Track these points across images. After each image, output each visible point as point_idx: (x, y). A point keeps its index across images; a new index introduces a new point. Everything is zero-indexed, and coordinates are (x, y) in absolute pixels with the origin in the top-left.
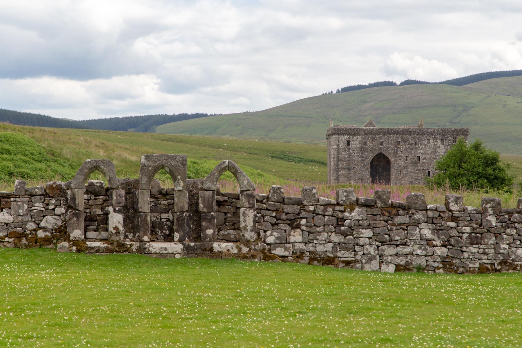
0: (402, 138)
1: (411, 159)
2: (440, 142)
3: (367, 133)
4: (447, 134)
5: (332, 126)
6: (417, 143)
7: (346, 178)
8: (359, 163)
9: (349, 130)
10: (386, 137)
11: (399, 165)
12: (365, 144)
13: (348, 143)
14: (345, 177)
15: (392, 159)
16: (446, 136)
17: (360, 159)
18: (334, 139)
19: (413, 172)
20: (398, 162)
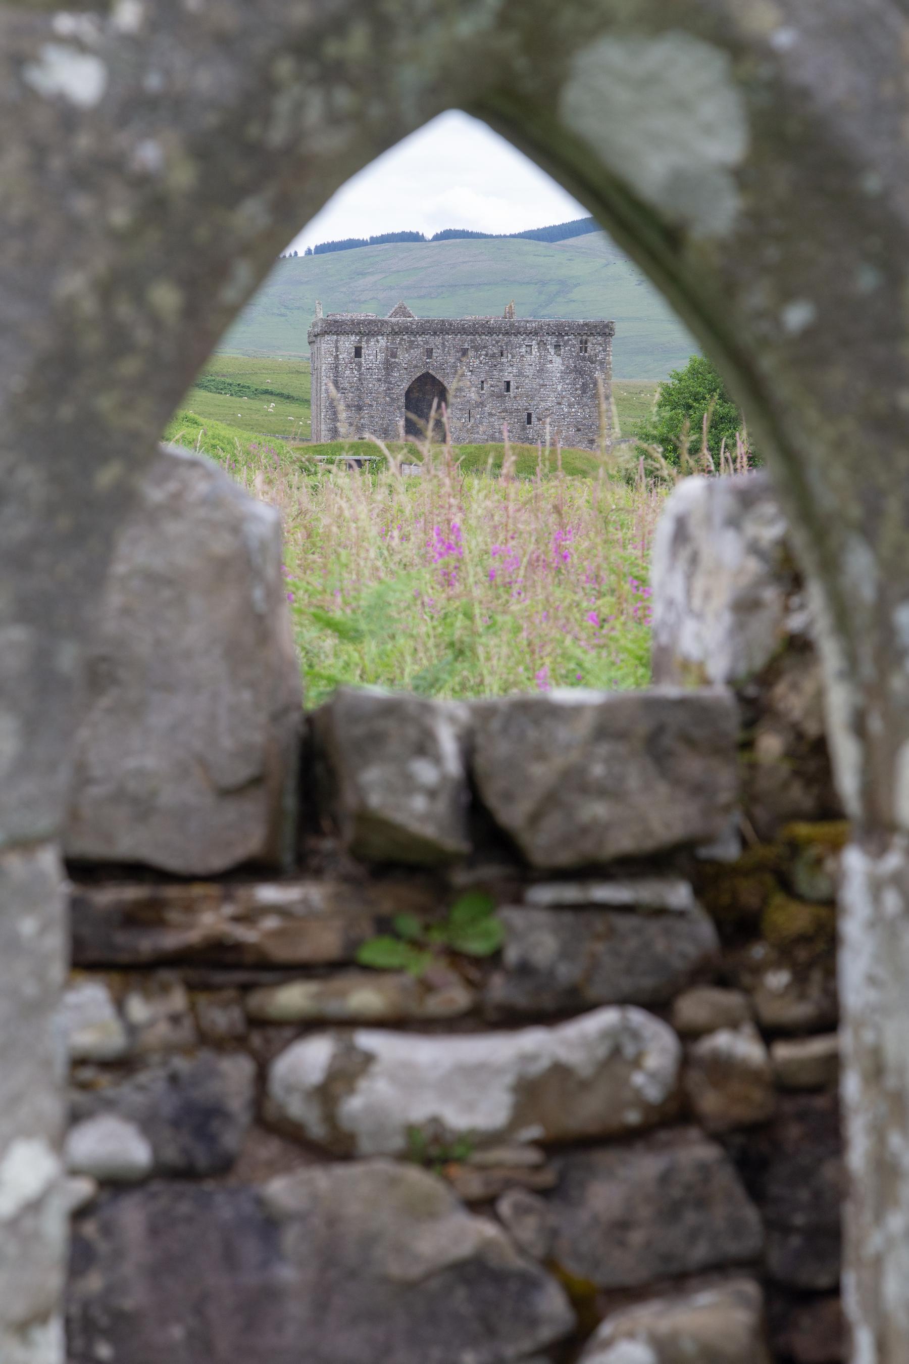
0: (471, 341)
1: (492, 386)
2: (552, 351)
3: (397, 331)
4: (567, 334)
5: (321, 315)
6: (505, 352)
9: (359, 324)
10: (438, 340)
11: (466, 399)
12: (394, 355)
13: (358, 352)
16: (566, 338)
17: (383, 387)
18: (326, 344)
19: (495, 415)
20: (463, 394)
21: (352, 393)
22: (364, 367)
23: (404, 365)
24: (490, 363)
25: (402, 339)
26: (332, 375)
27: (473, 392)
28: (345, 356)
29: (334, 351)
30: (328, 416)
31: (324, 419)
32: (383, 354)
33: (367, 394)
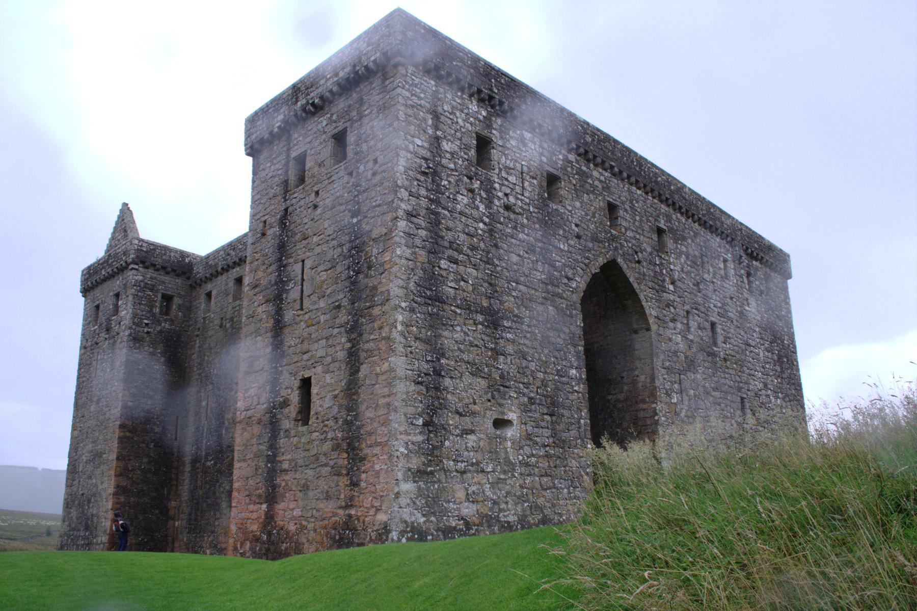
1: (699, 328)
7: (483, 383)
8: (538, 295)
15: (652, 311)
21: (475, 266)
22: (499, 199)
23: (573, 226)
24: (693, 275)
26: (423, 192)
27: (680, 334)
28: (456, 149)
29: (430, 122)
30: (414, 329)
32: (535, 182)
33: (509, 282)
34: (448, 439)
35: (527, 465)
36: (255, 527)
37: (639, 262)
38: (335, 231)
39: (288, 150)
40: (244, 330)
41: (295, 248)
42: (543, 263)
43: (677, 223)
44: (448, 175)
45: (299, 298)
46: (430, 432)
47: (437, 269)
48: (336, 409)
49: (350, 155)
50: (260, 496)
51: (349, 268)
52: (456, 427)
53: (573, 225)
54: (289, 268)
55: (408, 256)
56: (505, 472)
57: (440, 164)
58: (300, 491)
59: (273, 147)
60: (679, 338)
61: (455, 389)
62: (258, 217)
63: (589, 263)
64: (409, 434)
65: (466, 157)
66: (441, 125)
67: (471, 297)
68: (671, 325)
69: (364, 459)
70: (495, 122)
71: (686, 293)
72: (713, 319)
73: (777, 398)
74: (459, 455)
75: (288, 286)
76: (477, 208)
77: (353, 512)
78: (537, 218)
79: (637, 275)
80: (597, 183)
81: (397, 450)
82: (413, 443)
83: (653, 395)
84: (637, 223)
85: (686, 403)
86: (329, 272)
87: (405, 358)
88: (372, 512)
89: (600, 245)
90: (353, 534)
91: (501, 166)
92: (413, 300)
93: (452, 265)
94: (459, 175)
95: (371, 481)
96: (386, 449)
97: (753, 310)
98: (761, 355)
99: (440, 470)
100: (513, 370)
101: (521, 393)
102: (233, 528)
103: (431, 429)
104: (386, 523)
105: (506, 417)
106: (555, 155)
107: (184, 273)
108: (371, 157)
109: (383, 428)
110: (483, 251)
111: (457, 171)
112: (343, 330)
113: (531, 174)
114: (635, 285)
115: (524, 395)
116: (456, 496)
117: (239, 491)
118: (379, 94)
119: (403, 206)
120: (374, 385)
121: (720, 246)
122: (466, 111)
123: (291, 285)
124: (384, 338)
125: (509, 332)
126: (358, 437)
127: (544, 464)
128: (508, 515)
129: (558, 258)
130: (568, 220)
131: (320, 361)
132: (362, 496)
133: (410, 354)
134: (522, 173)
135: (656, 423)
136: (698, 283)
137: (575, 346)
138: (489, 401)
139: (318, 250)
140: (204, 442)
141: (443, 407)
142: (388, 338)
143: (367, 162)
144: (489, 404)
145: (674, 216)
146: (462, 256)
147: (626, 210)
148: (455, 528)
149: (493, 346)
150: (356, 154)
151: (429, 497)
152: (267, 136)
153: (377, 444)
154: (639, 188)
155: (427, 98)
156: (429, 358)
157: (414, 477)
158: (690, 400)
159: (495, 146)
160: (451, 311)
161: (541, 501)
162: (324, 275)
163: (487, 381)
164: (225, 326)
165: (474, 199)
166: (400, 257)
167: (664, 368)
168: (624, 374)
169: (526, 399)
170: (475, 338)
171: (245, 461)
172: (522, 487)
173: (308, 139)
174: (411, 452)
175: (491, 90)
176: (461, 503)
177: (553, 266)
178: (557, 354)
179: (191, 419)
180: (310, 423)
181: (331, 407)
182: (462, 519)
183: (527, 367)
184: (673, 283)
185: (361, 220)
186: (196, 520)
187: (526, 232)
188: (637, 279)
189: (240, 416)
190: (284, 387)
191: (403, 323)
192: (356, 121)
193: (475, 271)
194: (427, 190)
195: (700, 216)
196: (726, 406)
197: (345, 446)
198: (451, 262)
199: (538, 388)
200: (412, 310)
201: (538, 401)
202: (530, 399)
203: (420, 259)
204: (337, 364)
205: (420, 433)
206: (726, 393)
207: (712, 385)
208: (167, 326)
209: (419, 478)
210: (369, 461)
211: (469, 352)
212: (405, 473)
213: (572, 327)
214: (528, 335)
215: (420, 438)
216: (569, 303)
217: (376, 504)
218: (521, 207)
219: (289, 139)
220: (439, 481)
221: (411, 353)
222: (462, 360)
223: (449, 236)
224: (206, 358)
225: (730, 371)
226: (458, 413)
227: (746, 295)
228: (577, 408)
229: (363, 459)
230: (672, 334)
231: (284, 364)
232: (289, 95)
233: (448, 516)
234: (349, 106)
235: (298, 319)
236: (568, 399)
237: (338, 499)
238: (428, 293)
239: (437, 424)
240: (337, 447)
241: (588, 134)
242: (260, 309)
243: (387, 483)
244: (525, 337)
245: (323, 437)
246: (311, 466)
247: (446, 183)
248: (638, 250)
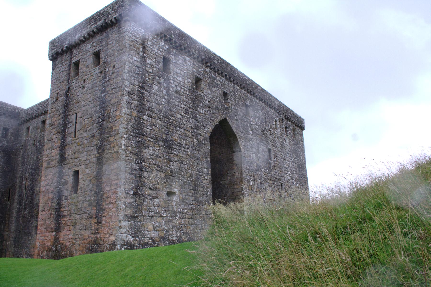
1: (263, 151)
7: (163, 174)
14: (159, 169)
15: (242, 143)
22: (173, 88)
23: (207, 102)
25: (205, 71)
26: (136, 83)
27: (254, 154)
28: (153, 63)
29: (141, 49)
30: (130, 148)
31: (124, 150)
32: (190, 80)
34: (145, 201)
35: (182, 213)
36: (49, 244)
37: (237, 120)
38: (93, 100)
39: (71, 59)
40: (46, 147)
41: (72, 107)
42: (192, 119)
43: (255, 103)
44: (149, 75)
45: (74, 131)
46: (136, 197)
47: (142, 120)
48: (91, 186)
49: (102, 63)
50: (52, 228)
51: (99, 118)
52: (149, 195)
53: (207, 102)
54: (69, 117)
55: (128, 113)
56: (172, 217)
57: (145, 69)
58: (72, 226)
59: (63, 57)
60: (254, 156)
61: (149, 177)
62: (54, 91)
63: (214, 120)
64: (126, 198)
65: (158, 67)
66: (146, 51)
67: (158, 134)
68: (251, 149)
69: (104, 210)
70: (173, 51)
71: (258, 135)
72: (270, 147)
73: (297, 183)
74: (150, 209)
75: (69, 125)
76: (162, 92)
77: (98, 236)
78: (190, 98)
79: (235, 126)
80: (219, 82)
81: (120, 206)
82: (128, 203)
83: (241, 182)
84: (236, 102)
85: (256, 185)
86: (89, 119)
87: (125, 162)
88: (108, 236)
89: (219, 111)
90: (98, 246)
91: (174, 72)
92: (130, 134)
93: (149, 118)
94: (154, 75)
95: (108, 221)
96: (115, 205)
97: (287, 144)
98: (290, 164)
99: (141, 215)
100: (177, 169)
101: (180, 179)
102: (38, 244)
103: (137, 196)
104: (114, 241)
105: (173, 191)
106: (200, 68)
107: (15, 117)
108: (112, 65)
109: (114, 195)
110: (164, 112)
111: (153, 74)
112: (95, 147)
113: (188, 77)
114: (235, 131)
115: (182, 180)
116: (149, 228)
117: (41, 226)
118: (117, 34)
119: (127, 89)
120: (110, 174)
121: (274, 114)
122: (158, 45)
123: (70, 125)
124: (115, 152)
125: (175, 151)
126: (102, 199)
127: (190, 213)
128: (173, 237)
129: (199, 117)
130: (205, 99)
131: (83, 162)
132: (103, 228)
133: (128, 160)
134: (184, 76)
135: (243, 194)
136: (263, 130)
137: (206, 158)
138: (165, 183)
139: (84, 108)
140: (24, 202)
141: (143, 185)
142: (117, 152)
143: (110, 67)
144: (165, 184)
145: (253, 100)
146: (154, 114)
147: (232, 96)
148: (148, 243)
149: (167, 157)
150: (104, 63)
151: (135, 228)
152: (60, 51)
153: (111, 203)
154: (238, 86)
155: (140, 38)
156: (137, 162)
157: (128, 219)
158: (258, 184)
159: (172, 62)
160: (148, 140)
161: (188, 230)
162: (87, 121)
163: (164, 173)
164: (36, 144)
165: (161, 87)
166: (124, 113)
167: (247, 169)
168: (229, 172)
169: (182, 183)
170: (159, 153)
171: (44, 211)
172: (179, 224)
173: (81, 54)
174: (127, 207)
175: (171, 36)
176: (151, 231)
177: (197, 120)
178: (197, 161)
179: (17, 190)
180: (78, 193)
181: (88, 185)
182: (151, 239)
183: (183, 167)
184: (252, 130)
185: (106, 95)
186: (18, 241)
187: (185, 104)
188: (236, 128)
189: (42, 189)
190: (65, 175)
191: (125, 145)
192: (105, 47)
193: (160, 121)
194: (139, 82)
195: (265, 100)
196: (274, 187)
197: (95, 204)
198: (148, 117)
199: (188, 177)
200: (129, 139)
201: (188, 184)
202: (184, 182)
203: (134, 115)
204: (92, 164)
205: (132, 198)
206: (274, 181)
207: (268, 178)
208: (5, 143)
209: (131, 219)
210: (107, 211)
211: (156, 159)
212: (124, 217)
213: (205, 149)
214: (184, 153)
215: (132, 200)
216: (204, 138)
217: (110, 232)
218: (183, 92)
219: (71, 53)
220: (140, 221)
221: (128, 159)
222: (153, 163)
223: (148, 104)
224: (26, 160)
225: (277, 171)
226: (150, 188)
227: (285, 137)
228: (206, 187)
229: (104, 210)
230: (251, 154)
231: (66, 163)
232: (72, 32)
233: (145, 237)
234: (102, 39)
235: (73, 142)
236: (202, 183)
237: (91, 229)
238: (137, 131)
239: (140, 194)
240: (91, 205)
241: (215, 59)
242: (54, 136)
243: (115, 222)
244: (183, 153)
245: (84, 199)
246: (78, 214)
247: (148, 79)
248: (236, 114)
